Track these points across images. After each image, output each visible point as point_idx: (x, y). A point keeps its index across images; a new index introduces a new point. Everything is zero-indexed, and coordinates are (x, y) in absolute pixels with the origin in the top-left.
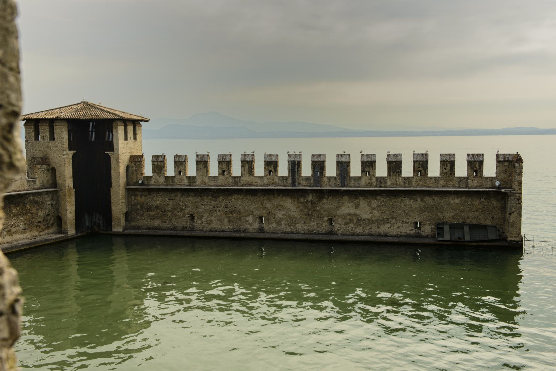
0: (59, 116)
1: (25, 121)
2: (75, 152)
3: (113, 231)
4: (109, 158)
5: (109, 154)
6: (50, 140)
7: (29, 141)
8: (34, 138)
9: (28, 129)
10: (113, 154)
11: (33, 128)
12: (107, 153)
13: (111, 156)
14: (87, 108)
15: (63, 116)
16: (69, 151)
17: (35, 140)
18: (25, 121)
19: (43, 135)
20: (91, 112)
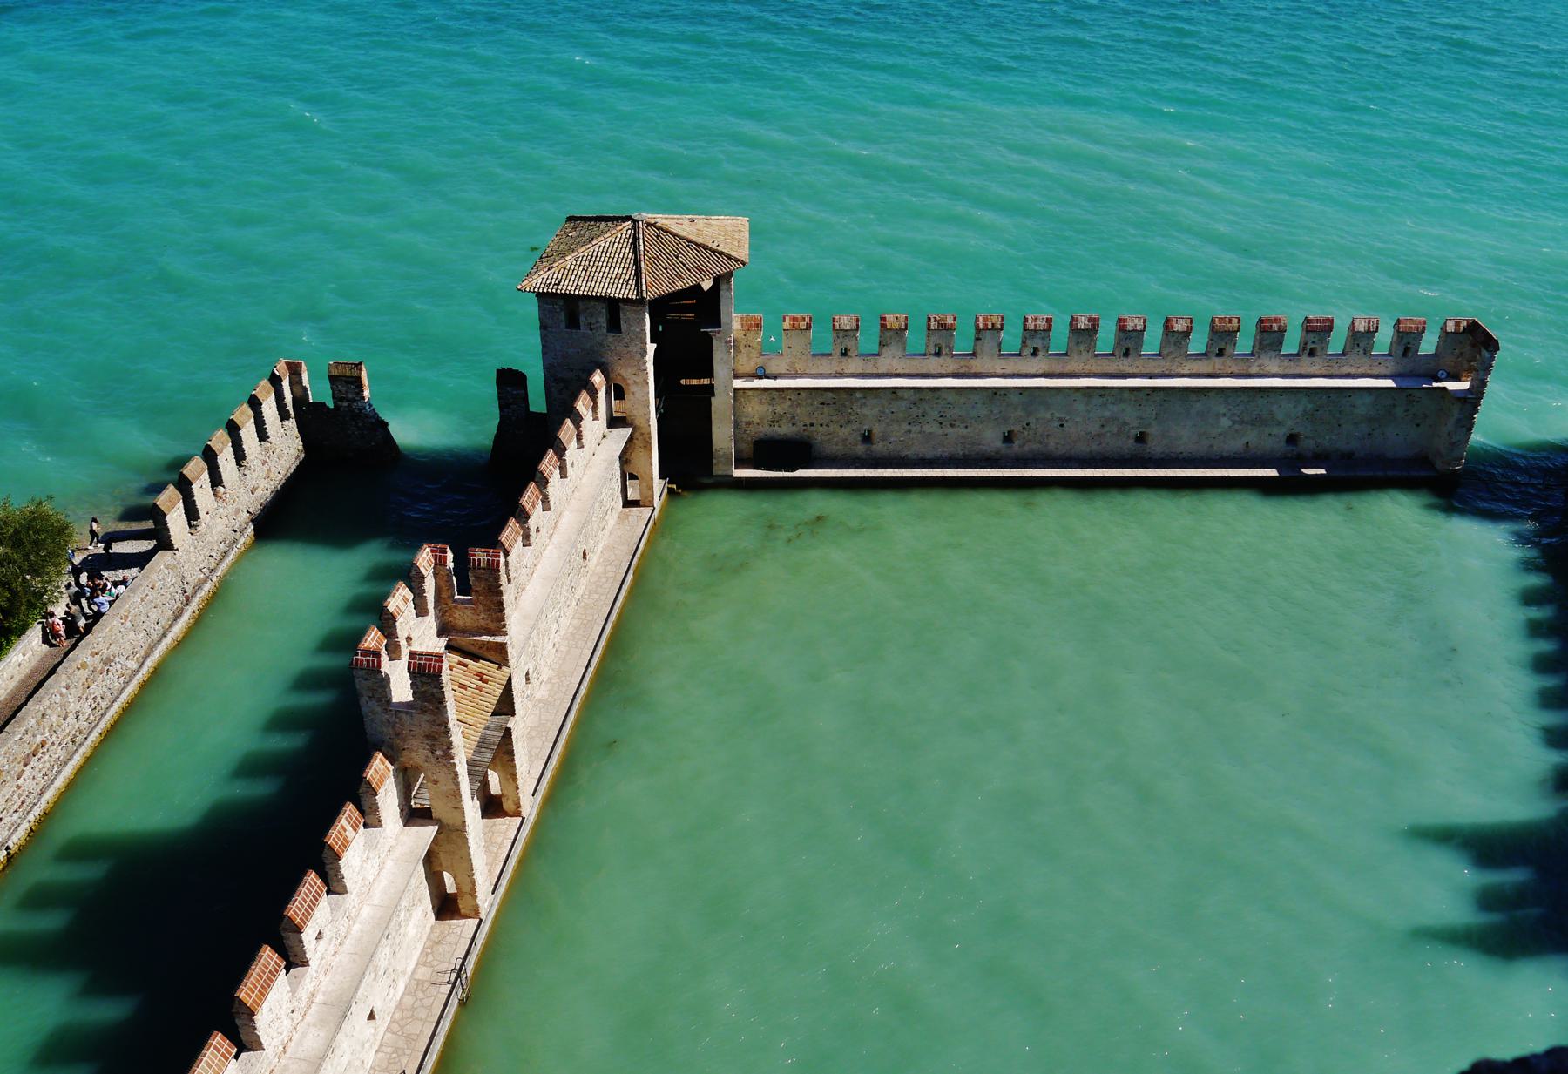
3: (714, 474)
4: (708, 342)
6: (609, 331)
8: (563, 325)
10: (719, 333)
12: (707, 332)
17: (567, 327)
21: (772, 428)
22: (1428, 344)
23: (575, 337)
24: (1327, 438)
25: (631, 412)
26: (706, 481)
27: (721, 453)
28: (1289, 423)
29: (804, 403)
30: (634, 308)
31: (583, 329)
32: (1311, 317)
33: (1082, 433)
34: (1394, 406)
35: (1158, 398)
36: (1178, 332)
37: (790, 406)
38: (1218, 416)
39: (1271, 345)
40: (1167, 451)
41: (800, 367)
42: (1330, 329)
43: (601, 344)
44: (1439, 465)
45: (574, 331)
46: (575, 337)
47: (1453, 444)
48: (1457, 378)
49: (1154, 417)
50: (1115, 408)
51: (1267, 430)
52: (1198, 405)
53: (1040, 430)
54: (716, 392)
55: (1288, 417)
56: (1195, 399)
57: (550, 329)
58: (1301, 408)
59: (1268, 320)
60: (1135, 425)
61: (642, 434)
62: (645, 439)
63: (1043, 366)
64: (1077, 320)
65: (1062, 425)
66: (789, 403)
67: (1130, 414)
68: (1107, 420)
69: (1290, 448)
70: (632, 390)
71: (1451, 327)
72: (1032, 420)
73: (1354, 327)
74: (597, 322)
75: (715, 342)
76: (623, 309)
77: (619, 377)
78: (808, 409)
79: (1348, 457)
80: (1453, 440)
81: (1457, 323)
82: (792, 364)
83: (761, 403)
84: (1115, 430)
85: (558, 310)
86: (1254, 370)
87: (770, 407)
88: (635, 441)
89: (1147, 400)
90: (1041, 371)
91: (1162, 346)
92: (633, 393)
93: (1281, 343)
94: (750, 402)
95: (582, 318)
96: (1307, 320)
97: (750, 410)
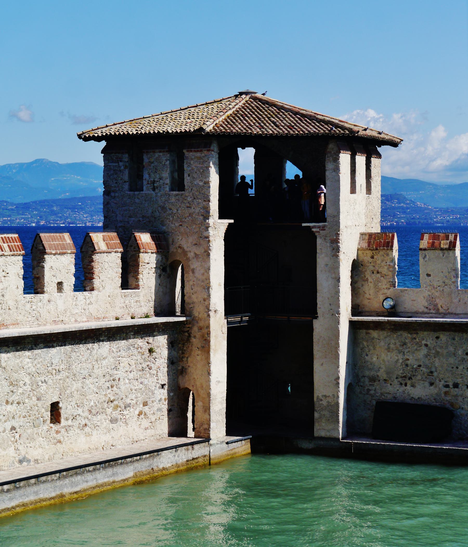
0: (204, 127)
1: (103, 144)
2: (232, 221)
3: (316, 434)
5: (314, 230)
6: (172, 189)
7: (113, 194)
8: (126, 186)
9: (113, 162)
10: (323, 228)
11: (126, 160)
13: (317, 234)
14: (257, 107)
15: (211, 128)
16: (220, 218)
17: (131, 190)
18: (103, 144)
19: (152, 175)
20: (273, 119)
21: (403, 388)
23: (137, 201)
25: (190, 297)
26: (306, 445)
27: (324, 403)
29: (445, 352)
30: (198, 154)
31: (147, 190)
37: (426, 356)
41: (440, 302)
43: (163, 208)
45: (136, 193)
46: (137, 201)
54: (319, 311)
57: (113, 194)
61: (200, 329)
62: (203, 336)
66: (424, 351)
70: (192, 267)
74: (161, 178)
75: (319, 241)
76: (187, 158)
77: (180, 251)
78: (451, 360)
82: (431, 299)
83: (389, 349)
85: (122, 168)
87: (400, 356)
88: (193, 340)
92: (193, 271)
94: (374, 349)
95: (146, 176)
97: (375, 359)
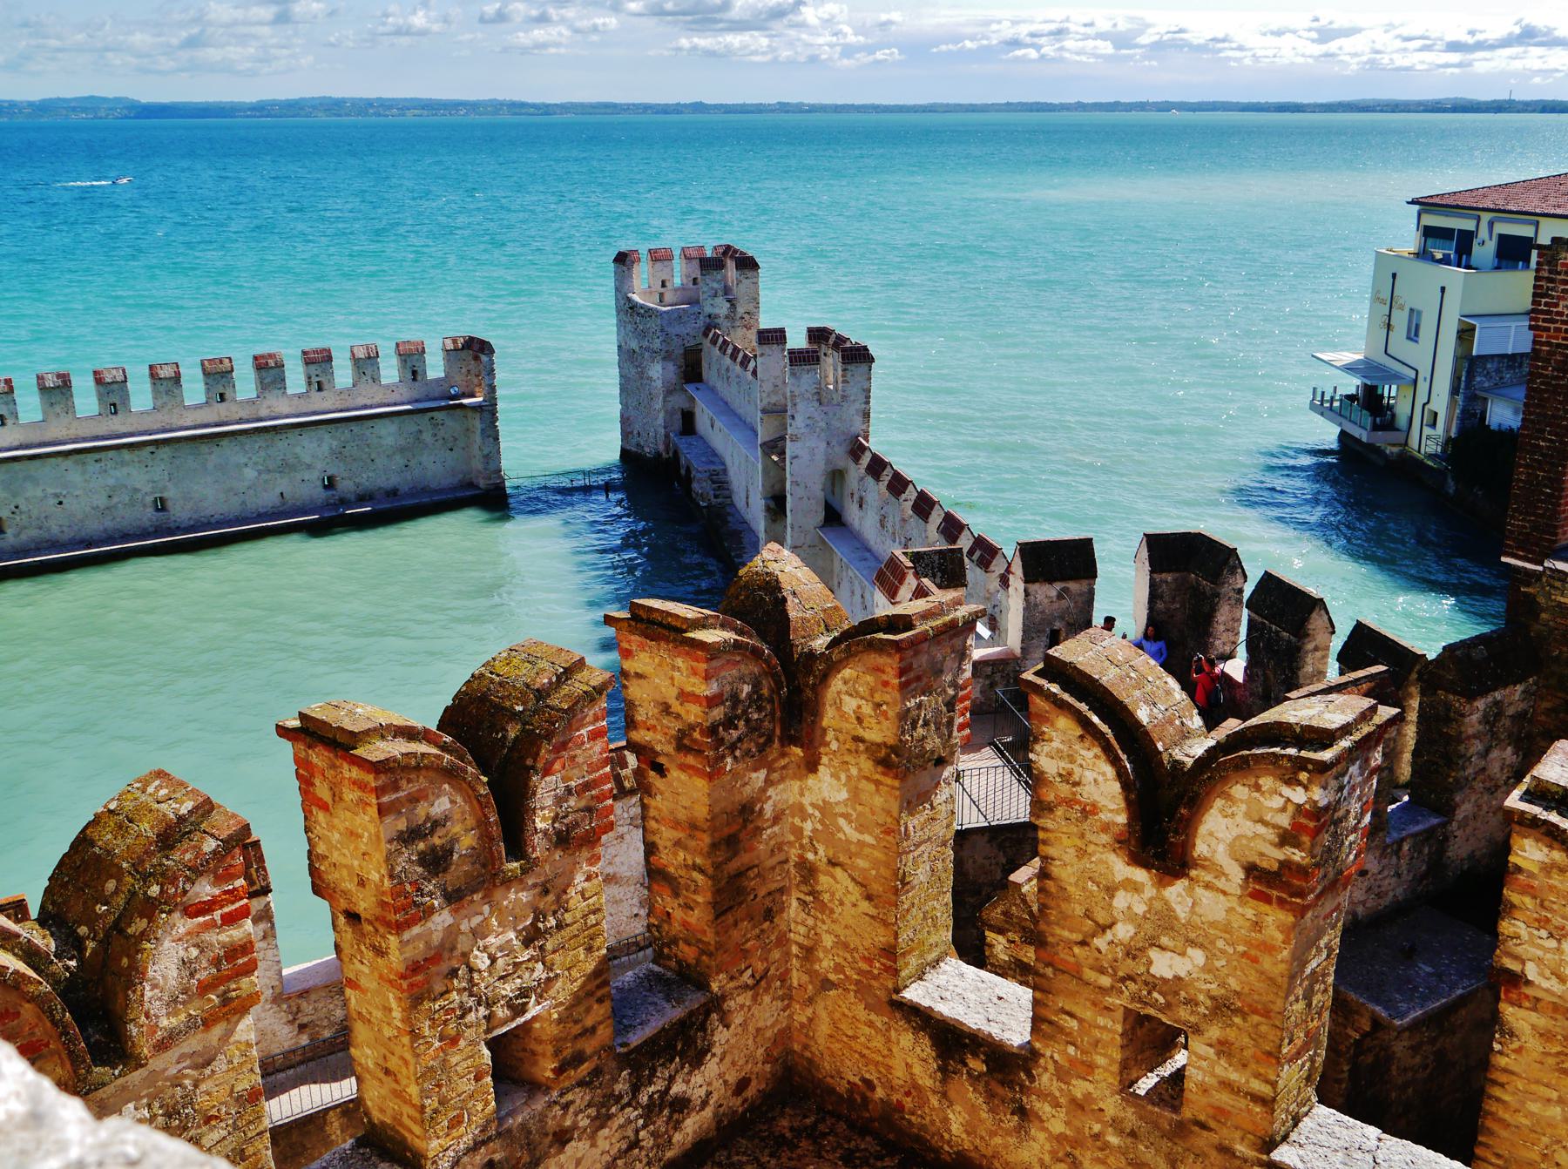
22: (435, 368)
24: (365, 476)
28: (320, 465)
32: (307, 349)
33: (88, 509)
34: (420, 431)
35: (165, 456)
36: (166, 379)
38: (238, 465)
39: (274, 382)
40: (195, 516)
42: (330, 359)
44: (482, 483)
47: (487, 457)
48: (473, 396)
49: (167, 478)
50: (118, 473)
51: (299, 477)
52: (213, 457)
53: (35, 513)
55: (315, 454)
56: (207, 450)
58: (325, 447)
59: (262, 357)
60: (148, 489)
63: (18, 436)
64: (43, 378)
65: (60, 503)
67: (142, 478)
68: (113, 489)
69: (330, 493)
71: (450, 346)
72: (21, 501)
73: (353, 354)
79: (393, 493)
80: (485, 452)
81: (455, 341)
84: (127, 499)
86: (264, 412)
89: (153, 460)
90: (16, 443)
91: (155, 398)
93: (283, 380)
96: (304, 353)
